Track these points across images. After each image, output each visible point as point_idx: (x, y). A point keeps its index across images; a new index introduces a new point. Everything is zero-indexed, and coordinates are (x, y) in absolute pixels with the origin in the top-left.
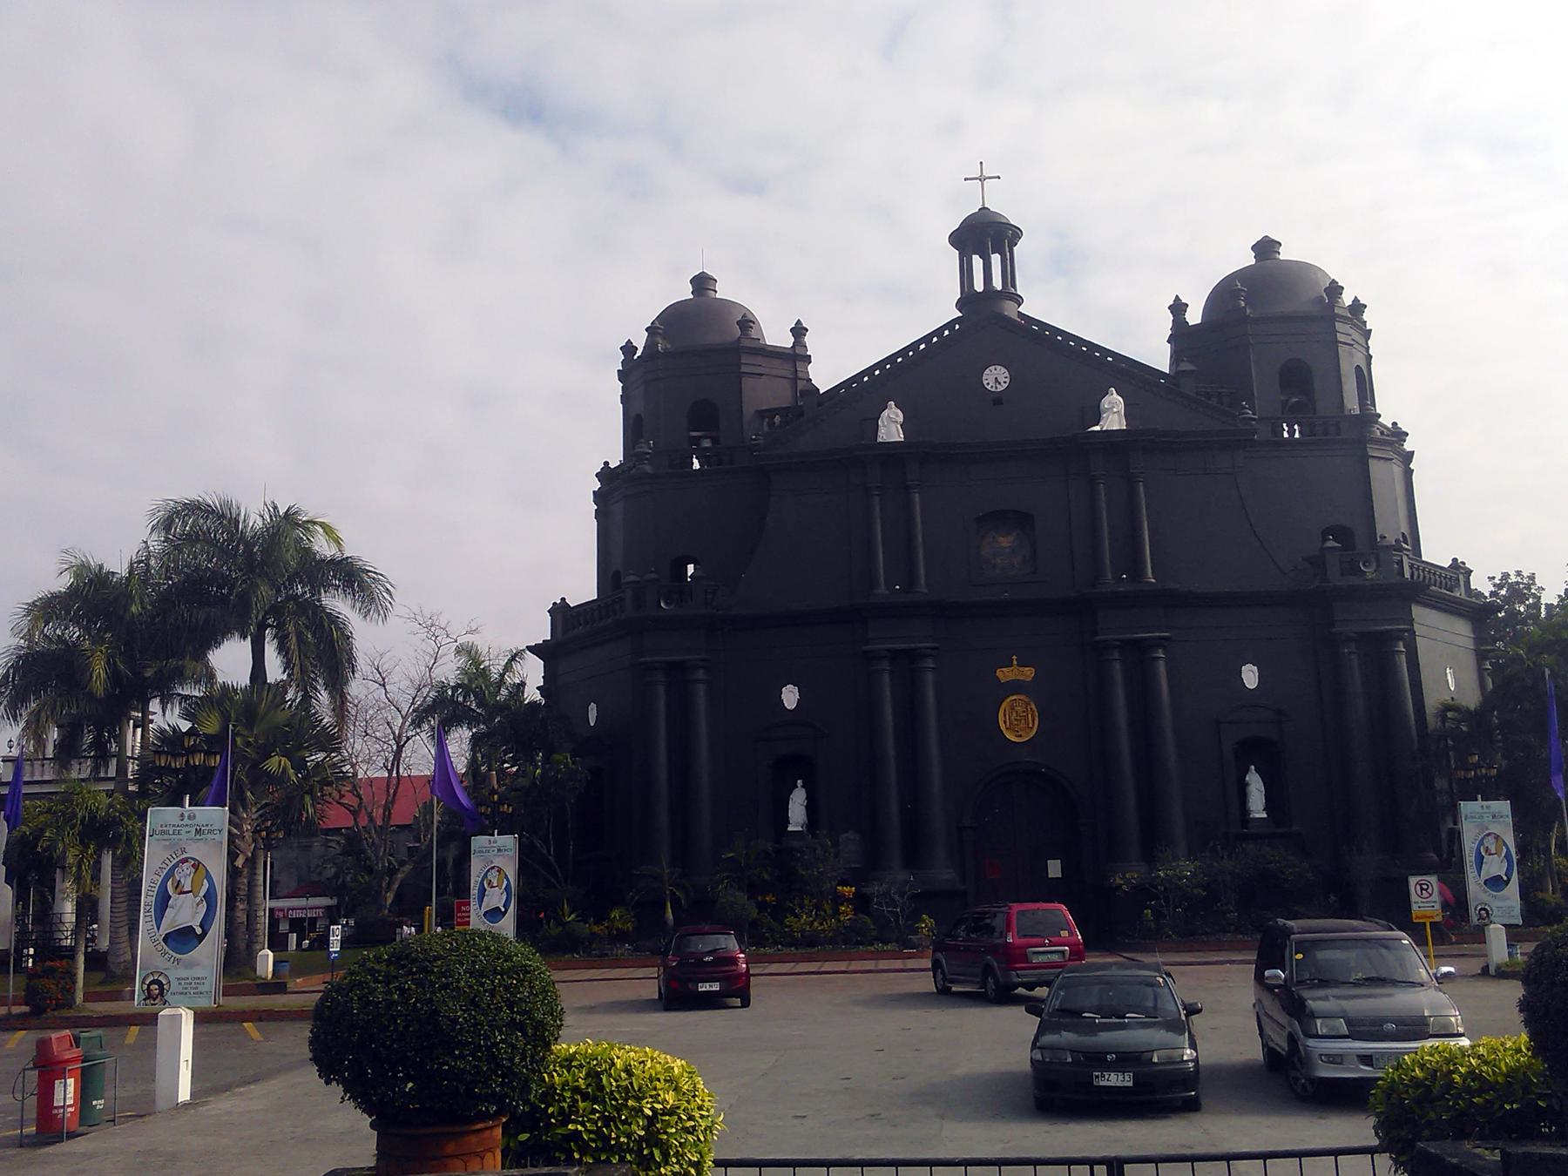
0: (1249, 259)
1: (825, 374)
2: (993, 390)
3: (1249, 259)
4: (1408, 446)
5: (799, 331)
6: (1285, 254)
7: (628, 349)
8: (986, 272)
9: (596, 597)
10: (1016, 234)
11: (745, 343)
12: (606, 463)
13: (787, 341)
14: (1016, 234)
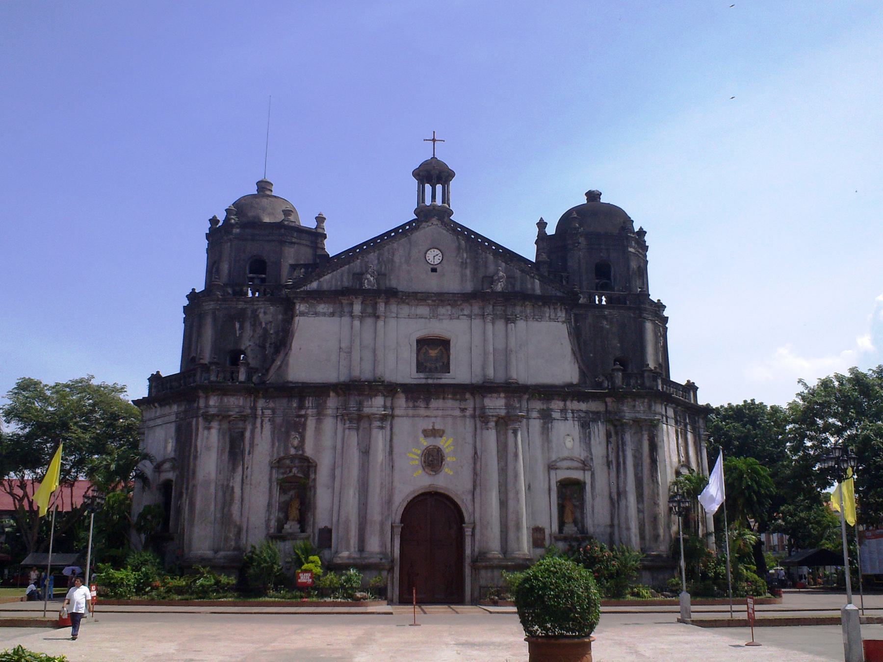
0: (584, 200)
1: (333, 247)
2: (432, 263)
3: (584, 200)
4: (666, 314)
5: (320, 219)
6: (604, 199)
7: (214, 221)
8: (433, 196)
9: (177, 371)
10: (450, 175)
12: (193, 290)
13: (312, 224)
14: (450, 175)
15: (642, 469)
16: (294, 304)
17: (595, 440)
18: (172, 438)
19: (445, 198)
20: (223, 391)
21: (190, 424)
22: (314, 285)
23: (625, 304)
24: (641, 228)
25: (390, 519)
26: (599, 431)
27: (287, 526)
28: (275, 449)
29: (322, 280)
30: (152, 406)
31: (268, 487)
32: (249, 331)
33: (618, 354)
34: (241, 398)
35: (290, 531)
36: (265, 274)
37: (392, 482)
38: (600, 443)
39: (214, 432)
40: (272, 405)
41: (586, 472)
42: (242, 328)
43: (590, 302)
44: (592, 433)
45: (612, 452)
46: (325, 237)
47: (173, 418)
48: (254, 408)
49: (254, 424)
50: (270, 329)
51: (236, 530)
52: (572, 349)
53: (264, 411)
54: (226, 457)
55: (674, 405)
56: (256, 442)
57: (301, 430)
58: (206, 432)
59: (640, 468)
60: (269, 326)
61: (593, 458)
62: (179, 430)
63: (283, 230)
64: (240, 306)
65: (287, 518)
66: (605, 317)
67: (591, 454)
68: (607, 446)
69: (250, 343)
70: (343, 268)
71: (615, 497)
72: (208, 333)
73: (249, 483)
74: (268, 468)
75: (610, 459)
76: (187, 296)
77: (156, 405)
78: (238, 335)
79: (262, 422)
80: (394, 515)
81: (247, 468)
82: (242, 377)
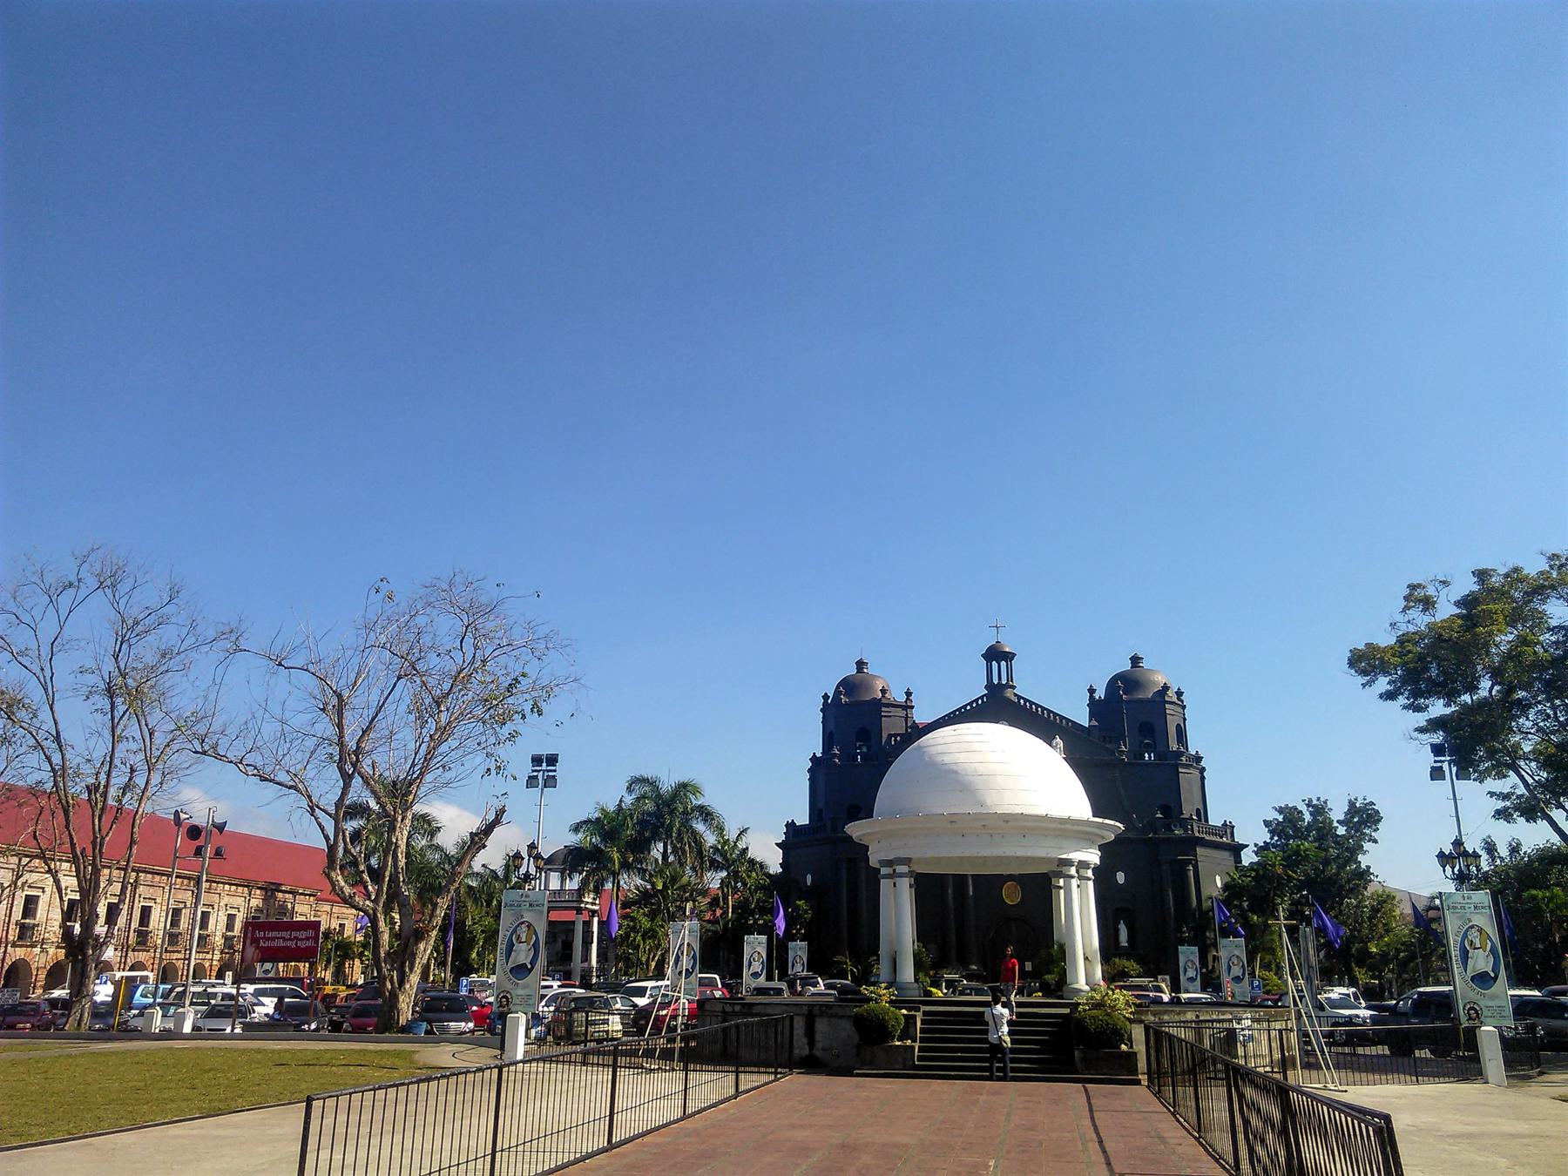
5: (909, 694)
7: (826, 697)
11: (884, 701)
13: (902, 698)
19: (1010, 677)
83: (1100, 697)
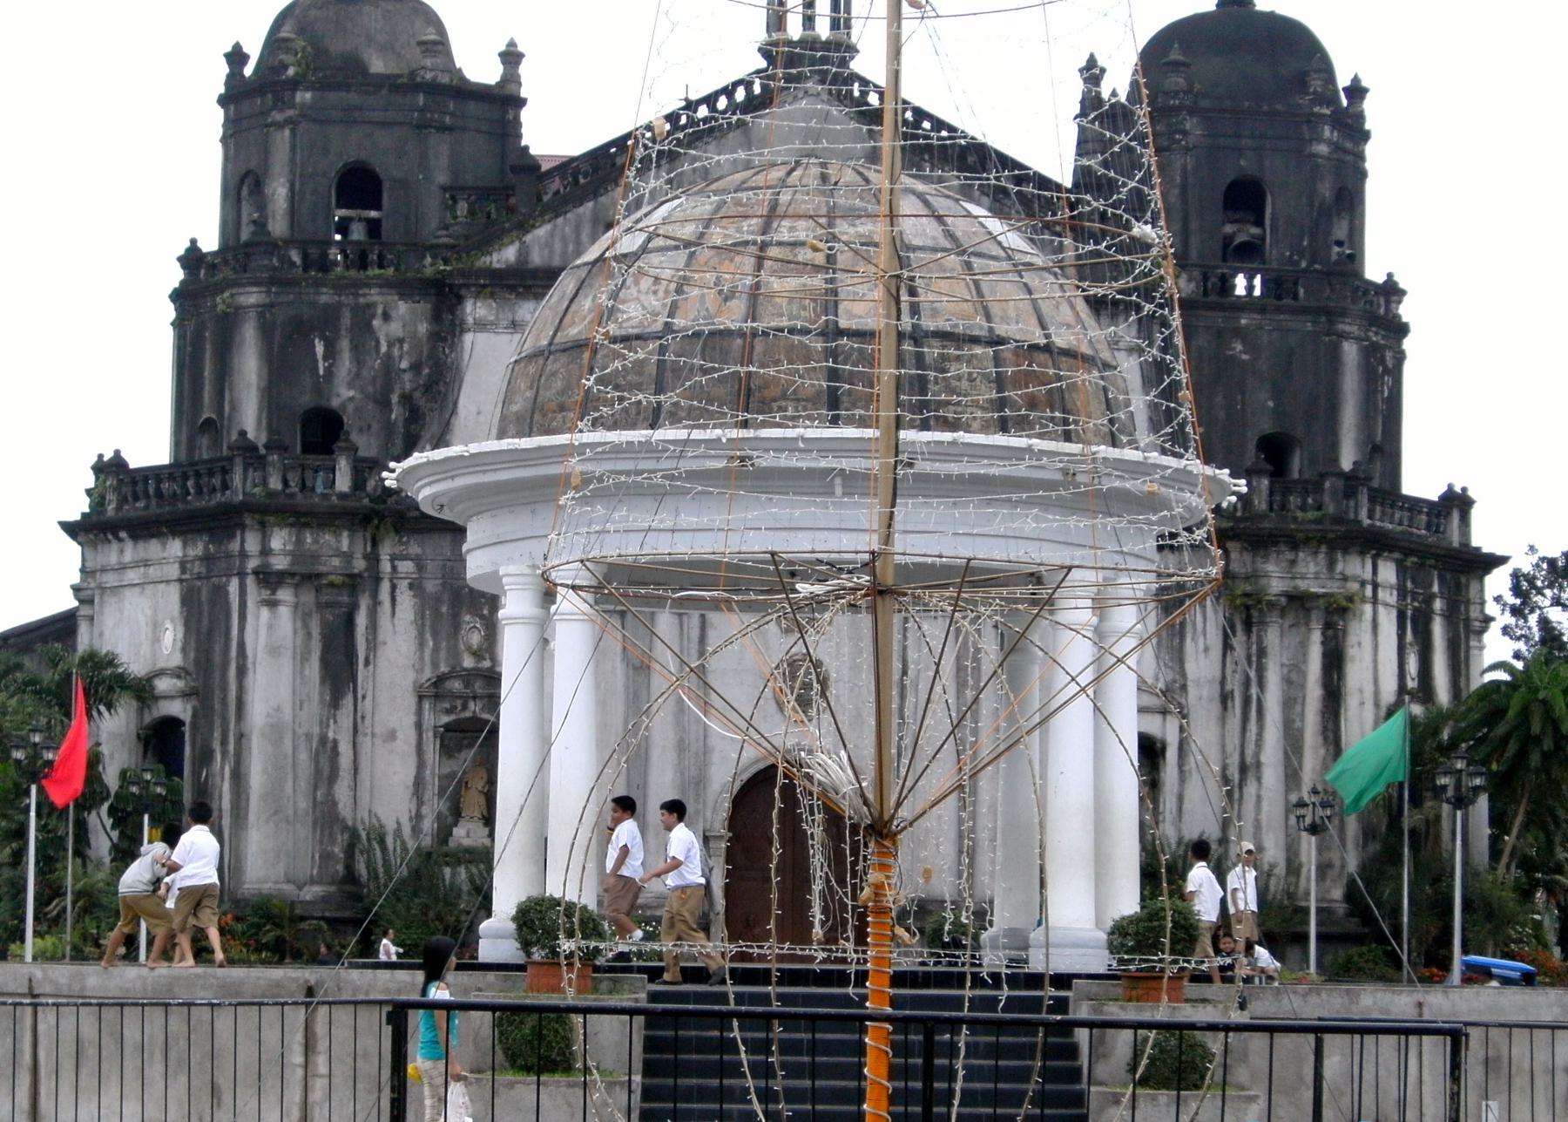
5: (511, 57)
7: (236, 57)
15: (1303, 711)
16: (460, 299)
17: (1196, 643)
18: (172, 620)
20: (300, 517)
21: (220, 593)
22: (508, 254)
23: (1295, 297)
24: (1356, 80)
25: (701, 820)
26: (1207, 623)
27: (459, 832)
28: (427, 658)
29: (528, 238)
30: (110, 537)
31: (414, 742)
32: (347, 363)
33: (1267, 426)
34: (345, 534)
35: (466, 842)
36: (378, 207)
37: (705, 737)
38: (1206, 650)
39: (284, 612)
40: (414, 549)
41: (1169, 717)
42: (331, 354)
43: (1205, 293)
44: (1189, 628)
45: (1234, 671)
46: (520, 103)
47: (174, 571)
48: (373, 559)
49: (375, 595)
50: (401, 357)
51: (346, 836)
52: (1150, 419)
53: (396, 562)
54: (314, 669)
55: (1397, 555)
56: (381, 638)
57: (485, 612)
58: (265, 613)
59: (1298, 708)
60: (396, 352)
61: (1189, 683)
62: (189, 600)
63: (421, 99)
64: (324, 299)
65: (457, 813)
66: (1238, 333)
67: (1183, 674)
68: (1224, 656)
69: (351, 393)
70: (581, 210)
71: (1234, 773)
72: (249, 367)
73: (369, 731)
74: (411, 701)
75: (1228, 687)
76: (180, 259)
77: (123, 534)
78: (321, 372)
79: (394, 588)
80: (709, 814)
81: (364, 697)
82: (343, 483)
83: (1114, 94)
